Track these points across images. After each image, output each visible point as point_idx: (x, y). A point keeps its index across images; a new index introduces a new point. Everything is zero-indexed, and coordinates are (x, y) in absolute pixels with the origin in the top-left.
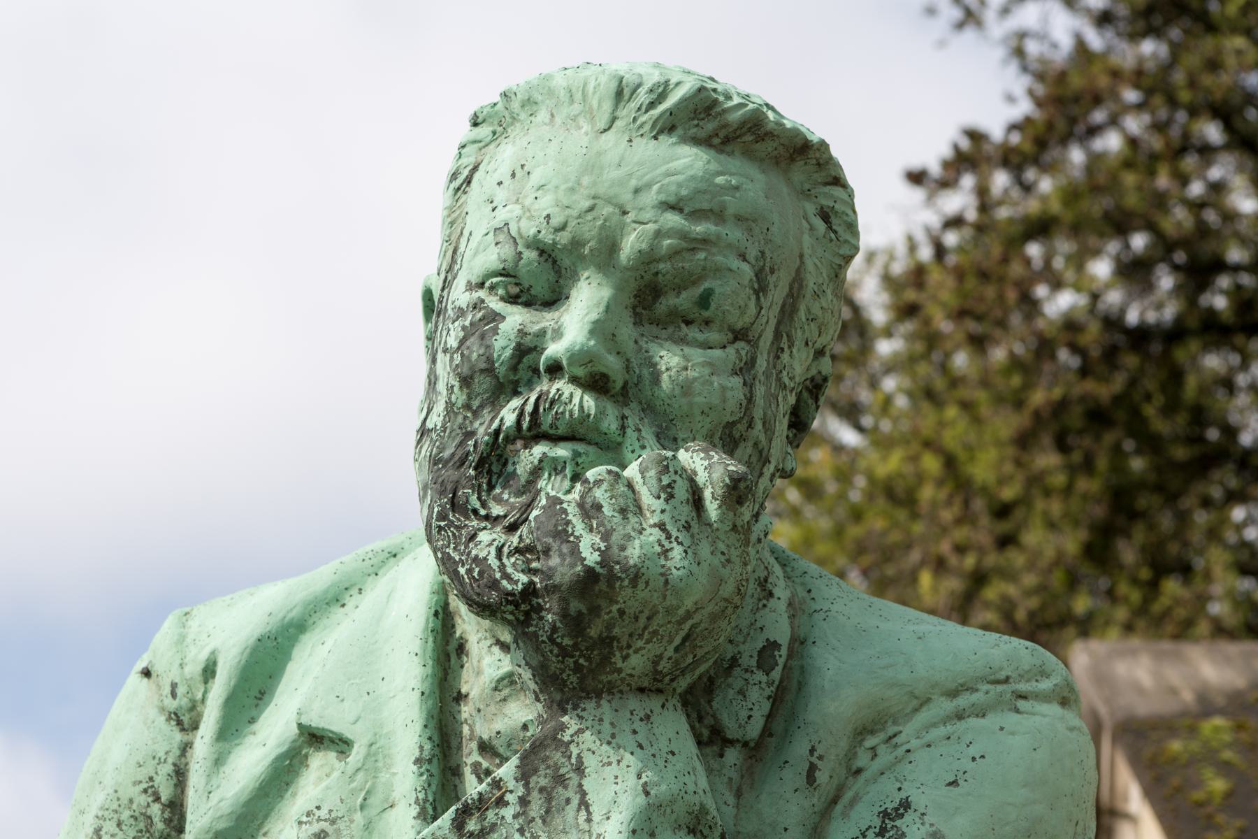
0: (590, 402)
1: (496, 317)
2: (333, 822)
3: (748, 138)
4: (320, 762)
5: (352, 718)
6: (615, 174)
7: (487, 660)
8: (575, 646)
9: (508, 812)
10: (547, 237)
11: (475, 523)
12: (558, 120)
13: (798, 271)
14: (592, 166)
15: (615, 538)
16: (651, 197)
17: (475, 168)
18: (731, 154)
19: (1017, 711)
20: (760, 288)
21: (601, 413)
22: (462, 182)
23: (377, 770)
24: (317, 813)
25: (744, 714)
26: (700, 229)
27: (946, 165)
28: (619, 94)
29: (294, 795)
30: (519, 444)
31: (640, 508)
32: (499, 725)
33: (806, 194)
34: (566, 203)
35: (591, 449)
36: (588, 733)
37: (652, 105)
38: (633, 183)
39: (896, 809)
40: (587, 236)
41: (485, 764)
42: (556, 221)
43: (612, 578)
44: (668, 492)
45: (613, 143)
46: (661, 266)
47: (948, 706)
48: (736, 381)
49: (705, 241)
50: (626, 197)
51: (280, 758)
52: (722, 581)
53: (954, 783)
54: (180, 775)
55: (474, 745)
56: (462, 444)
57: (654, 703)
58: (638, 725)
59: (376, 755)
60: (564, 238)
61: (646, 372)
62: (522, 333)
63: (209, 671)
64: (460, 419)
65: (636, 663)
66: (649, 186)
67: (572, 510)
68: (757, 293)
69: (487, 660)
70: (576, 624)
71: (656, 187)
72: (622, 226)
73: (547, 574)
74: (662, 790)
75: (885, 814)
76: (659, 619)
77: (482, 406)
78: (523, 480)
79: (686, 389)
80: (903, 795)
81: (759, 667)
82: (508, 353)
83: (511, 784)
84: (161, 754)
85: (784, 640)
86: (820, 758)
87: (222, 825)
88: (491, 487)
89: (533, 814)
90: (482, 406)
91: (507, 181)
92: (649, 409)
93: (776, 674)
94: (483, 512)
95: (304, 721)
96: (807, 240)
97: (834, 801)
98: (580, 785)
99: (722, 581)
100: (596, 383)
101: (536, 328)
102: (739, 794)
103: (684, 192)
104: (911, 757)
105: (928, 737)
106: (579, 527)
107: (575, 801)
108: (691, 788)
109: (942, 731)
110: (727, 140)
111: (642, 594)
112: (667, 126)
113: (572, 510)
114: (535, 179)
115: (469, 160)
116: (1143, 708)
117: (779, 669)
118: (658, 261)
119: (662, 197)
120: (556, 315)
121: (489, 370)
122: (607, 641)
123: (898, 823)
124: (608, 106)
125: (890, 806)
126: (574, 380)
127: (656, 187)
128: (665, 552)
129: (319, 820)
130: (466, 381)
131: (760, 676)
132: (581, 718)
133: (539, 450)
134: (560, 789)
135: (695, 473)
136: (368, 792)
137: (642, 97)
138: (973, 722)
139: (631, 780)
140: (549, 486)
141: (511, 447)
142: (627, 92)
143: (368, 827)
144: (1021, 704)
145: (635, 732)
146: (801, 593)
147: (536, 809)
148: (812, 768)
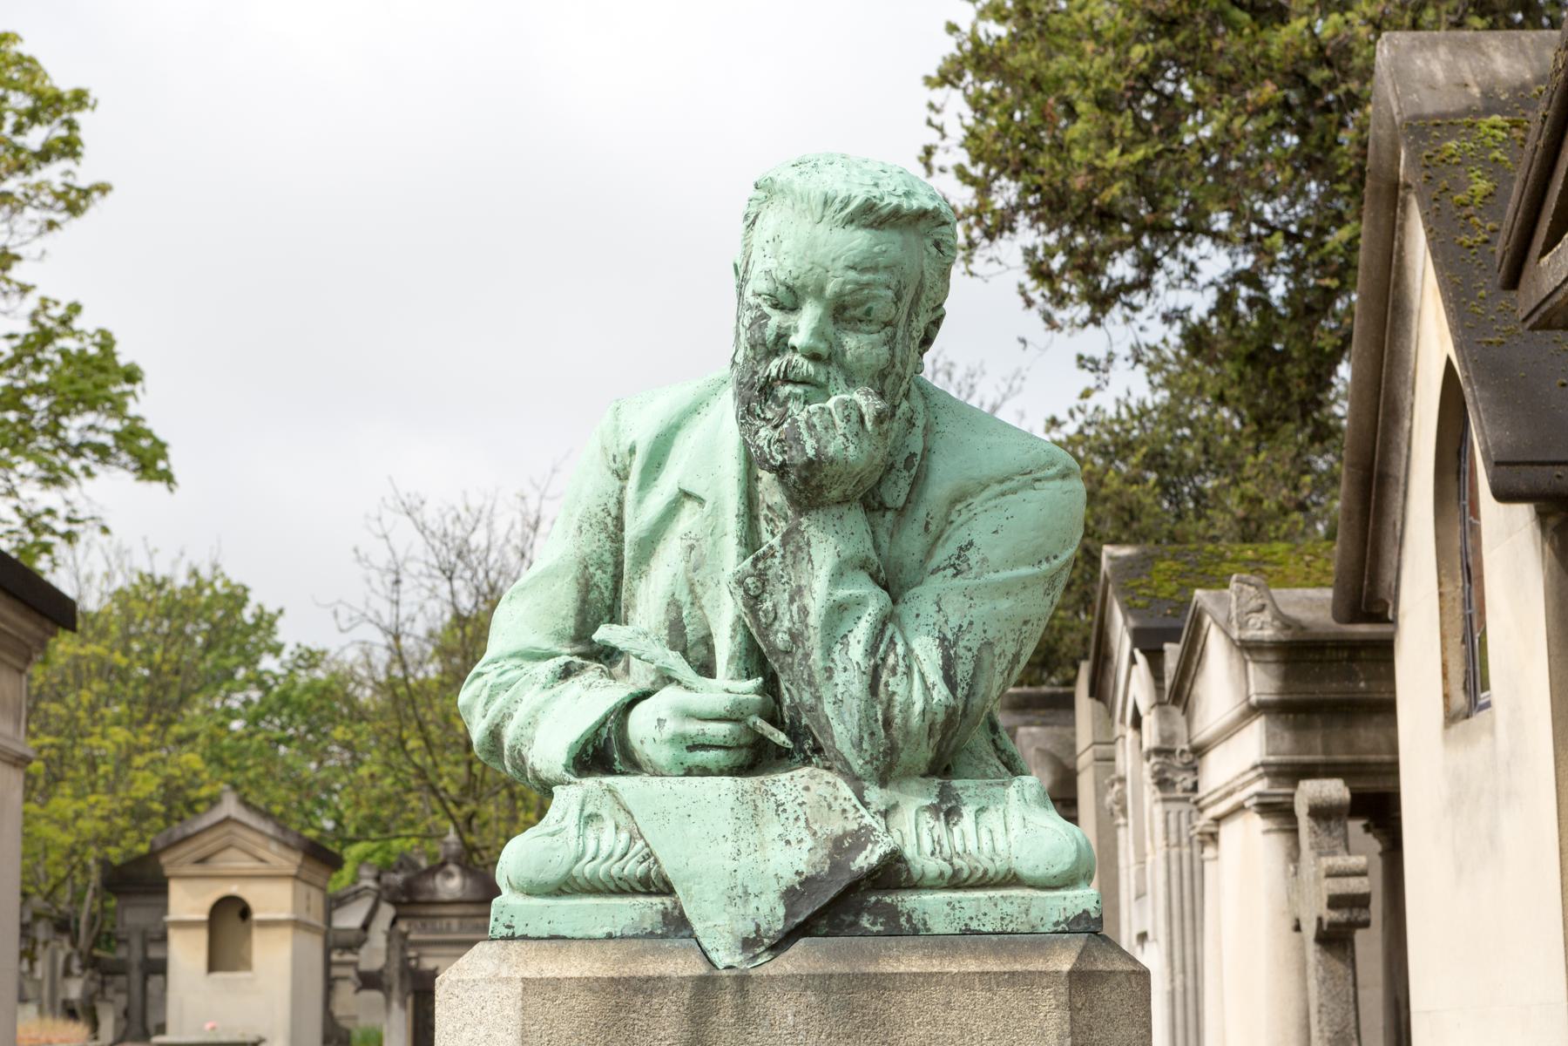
1: (765, 316)
4: (689, 505)
6: (822, 251)
9: (777, 561)
10: (790, 283)
11: (758, 423)
13: (920, 282)
14: (812, 246)
15: (822, 442)
16: (840, 263)
17: (756, 217)
18: (883, 230)
20: (898, 297)
21: (817, 373)
25: (896, 494)
26: (866, 277)
28: (825, 203)
33: (926, 235)
35: (813, 389)
37: (842, 209)
38: (832, 256)
42: (794, 274)
43: (820, 462)
44: (847, 419)
45: (822, 229)
47: (997, 488)
48: (886, 348)
49: (868, 285)
50: (828, 263)
51: (670, 503)
52: (874, 457)
53: (996, 532)
54: (620, 504)
56: (752, 377)
57: (845, 508)
58: (836, 522)
59: (717, 510)
60: (798, 283)
61: (839, 350)
62: (779, 327)
63: (632, 451)
65: (835, 493)
66: (840, 257)
67: (803, 425)
68: (896, 303)
70: (805, 481)
72: (827, 278)
73: (791, 458)
74: (846, 554)
79: (859, 359)
82: (772, 338)
83: (778, 548)
85: (919, 451)
87: (643, 535)
88: (766, 400)
92: (841, 366)
93: (913, 471)
96: (926, 261)
97: (939, 538)
99: (874, 457)
100: (814, 357)
101: (786, 325)
102: (891, 536)
103: (857, 260)
105: (986, 506)
106: (805, 435)
108: (861, 549)
109: (993, 503)
110: (881, 223)
111: (835, 468)
112: (850, 220)
113: (803, 425)
115: (753, 210)
116: (1431, 105)
121: (764, 344)
122: (820, 487)
124: (820, 209)
125: (964, 544)
130: (753, 347)
131: (905, 473)
137: (837, 205)
138: (1010, 497)
140: (793, 407)
143: (714, 544)
144: (1037, 485)
146: (932, 419)
147: (789, 560)
148: (927, 523)
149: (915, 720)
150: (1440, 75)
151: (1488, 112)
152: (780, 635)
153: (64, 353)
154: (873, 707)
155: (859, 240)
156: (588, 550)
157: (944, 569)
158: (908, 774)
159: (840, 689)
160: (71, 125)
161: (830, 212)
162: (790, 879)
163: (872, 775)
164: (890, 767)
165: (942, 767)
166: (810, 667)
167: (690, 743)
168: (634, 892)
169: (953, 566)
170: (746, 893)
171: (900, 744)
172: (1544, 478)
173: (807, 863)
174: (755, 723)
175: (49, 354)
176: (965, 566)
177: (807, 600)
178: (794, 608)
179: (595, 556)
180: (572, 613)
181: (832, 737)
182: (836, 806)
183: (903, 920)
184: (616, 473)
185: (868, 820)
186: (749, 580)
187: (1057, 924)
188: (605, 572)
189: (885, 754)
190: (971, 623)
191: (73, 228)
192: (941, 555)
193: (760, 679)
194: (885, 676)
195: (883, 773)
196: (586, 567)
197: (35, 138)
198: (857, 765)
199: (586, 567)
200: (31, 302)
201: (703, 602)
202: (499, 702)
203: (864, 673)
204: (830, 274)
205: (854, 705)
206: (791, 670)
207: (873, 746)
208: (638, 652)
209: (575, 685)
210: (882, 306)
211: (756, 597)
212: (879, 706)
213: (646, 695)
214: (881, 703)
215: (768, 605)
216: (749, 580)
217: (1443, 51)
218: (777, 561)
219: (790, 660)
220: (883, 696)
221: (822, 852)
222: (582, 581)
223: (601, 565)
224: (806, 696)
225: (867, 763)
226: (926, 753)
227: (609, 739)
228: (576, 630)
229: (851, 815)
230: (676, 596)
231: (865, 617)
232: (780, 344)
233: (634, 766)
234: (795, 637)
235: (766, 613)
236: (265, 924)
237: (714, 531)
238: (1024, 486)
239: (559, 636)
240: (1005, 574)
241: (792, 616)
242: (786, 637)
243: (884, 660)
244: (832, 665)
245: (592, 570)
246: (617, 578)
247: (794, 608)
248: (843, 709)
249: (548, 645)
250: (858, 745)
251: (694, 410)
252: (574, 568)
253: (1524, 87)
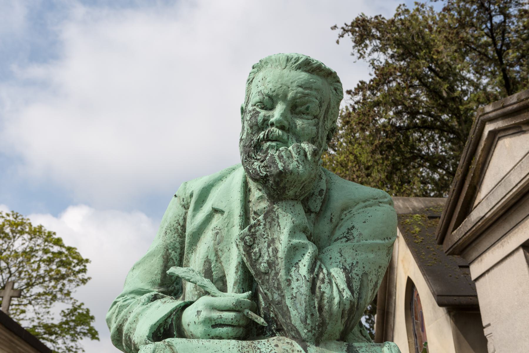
0: (280, 132)
1: (258, 113)
2: (220, 230)
3: (318, 71)
4: (217, 216)
5: (224, 206)
7: (256, 193)
8: (277, 189)
9: (261, 227)
10: (271, 94)
11: (253, 160)
12: (273, 66)
13: (329, 102)
14: (281, 77)
15: (286, 163)
16: (295, 84)
17: (253, 78)
18: (314, 74)
19: (379, 206)
20: (320, 106)
21: (283, 135)
22: (250, 82)
23: (230, 218)
24: (217, 228)
25: (315, 206)
27: (355, 89)
28: (287, 60)
29: (211, 224)
30: (264, 142)
31: (292, 157)
32: (259, 208)
33: (331, 84)
34: (275, 85)
35: (281, 143)
36: (280, 209)
37: (295, 63)
38: (291, 81)
39: (351, 228)
40: (280, 93)
41: (255, 217)
42: (273, 90)
43: (286, 173)
44: (299, 153)
46: (297, 100)
47: (363, 204)
48: (315, 128)
49: (308, 95)
50: (289, 84)
51: (208, 215)
52: (311, 174)
53: (365, 222)
54: (185, 219)
55: (253, 212)
56: (250, 142)
57: (295, 202)
58: (291, 207)
59: (230, 214)
60: (274, 94)
61: (294, 125)
62: (264, 116)
64: (250, 136)
65: (291, 193)
66: (294, 81)
68: (320, 107)
69: (256, 193)
70: (277, 184)
71: (296, 82)
72: (288, 91)
73: (270, 172)
74: (297, 222)
75: (349, 229)
76: (297, 183)
77: (255, 133)
78: (265, 151)
79: (303, 129)
80: (353, 225)
81: (319, 195)
82: (261, 121)
83: (262, 221)
84: (180, 214)
85: (325, 189)
86: (333, 216)
87: (194, 231)
88: (257, 152)
89: (267, 228)
90: (255, 133)
91: (261, 81)
92: (294, 134)
93: (323, 197)
94: (255, 158)
95: (213, 207)
96: (331, 95)
97: (336, 226)
98: (278, 221)
99: (311, 174)
100: (282, 128)
102: (314, 224)
103: (303, 83)
104: (354, 216)
105: (359, 212)
106: (278, 161)
107: (277, 225)
108: (304, 222)
109: (362, 210)
110: (313, 71)
111: (293, 177)
112: (299, 68)
114: (268, 80)
115: (252, 76)
117: (324, 196)
118: (297, 99)
119: (298, 84)
120: (273, 112)
121: (257, 125)
122: (284, 188)
123: (352, 231)
124: (285, 63)
125: (350, 227)
126: (277, 127)
127: (296, 82)
128: (298, 167)
129: (217, 229)
130: (251, 128)
131: (319, 197)
132: (278, 205)
133: (268, 143)
134: (273, 222)
135: (305, 149)
136: (228, 223)
137: (293, 61)
138: (369, 208)
139: (290, 220)
140: (271, 152)
141: (262, 143)
142: (289, 60)
143: (228, 231)
144: (380, 204)
145: (291, 209)
146: (329, 178)
147: (268, 226)
148: (331, 218)
149: (335, 307)
150: (401, 206)
151: (415, 214)
152: (262, 264)
153: (79, 313)
154: (313, 300)
155: (303, 76)
156: (169, 242)
157: (341, 239)
158: (330, 339)
159: (295, 290)
160: (85, 266)
161: (289, 64)
163: (311, 339)
164: (321, 334)
165: (343, 337)
166: (278, 280)
167: (213, 323)
169: (346, 237)
171: (327, 321)
172: (452, 300)
174: (248, 313)
175: (76, 313)
176: (351, 237)
178: (270, 250)
179: (172, 244)
180: (160, 272)
181: (290, 317)
184: (184, 206)
186: (247, 238)
188: (176, 252)
189: (319, 326)
190: (357, 263)
191: (82, 286)
192: (338, 233)
193: (250, 292)
194: (318, 284)
195: (318, 337)
196: (168, 250)
197: (77, 268)
198: (303, 332)
199: (168, 250)
200: (73, 301)
201: (222, 259)
202: (123, 313)
203: (308, 281)
204: (290, 88)
205: (303, 299)
206: (268, 282)
207: (312, 321)
208: (189, 278)
209: (158, 302)
210: (314, 106)
211: (250, 246)
212: (316, 299)
213: (191, 303)
214: (317, 298)
215: (256, 250)
216: (247, 238)
217: (401, 201)
219: (267, 277)
220: (318, 293)
222: (165, 257)
223: (174, 249)
224: (276, 296)
225: (309, 331)
226: (340, 327)
227: (172, 324)
228: (161, 280)
230: (209, 257)
231: (307, 254)
232: (265, 123)
233: (181, 334)
234: (271, 264)
235: (255, 254)
237: (229, 225)
238: (374, 204)
239: (153, 283)
240: (370, 242)
241: (269, 254)
242: (266, 265)
243: (318, 275)
244: (290, 278)
245: (170, 251)
247: (270, 250)
248: (296, 302)
249: (147, 287)
250: (304, 321)
251: (220, 179)
252: (162, 251)
253: (422, 208)
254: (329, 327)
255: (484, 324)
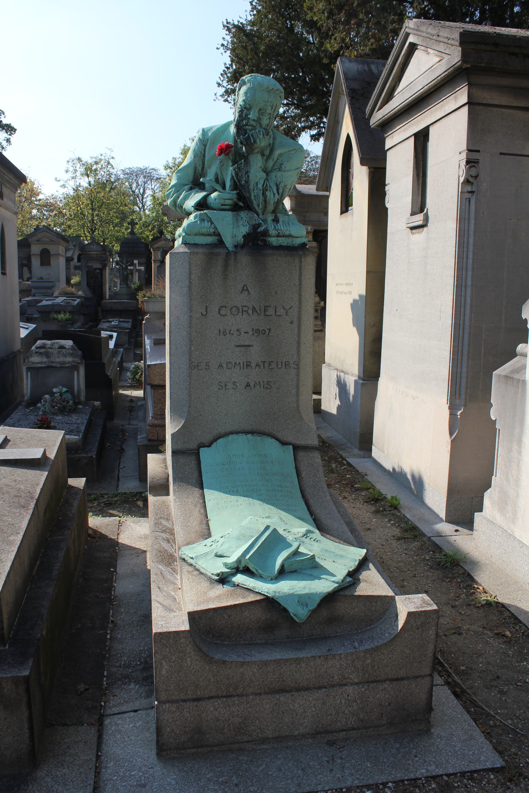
54: (205, 151)
65: (256, 151)
67: (251, 135)
106: (251, 138)
113: (251, 135)
122: (253, 149)
162: (244, 233)
168: (212, 235)
170: (236, 236)
173: (248, 230)
177: (249, 174)
178: (246, 175)
182: (254, 219)
183: (267, 243)
185: (260, 221)
187: (298, 245)
189: (264, 208)
216: (236, 169)
218: (243, 165)
221: (251, 228)
229: (257, 220)
236: (53, 255)
246: (203, 168)
247: (246, 175)
254: (268, 208)
255: (386, 183)
